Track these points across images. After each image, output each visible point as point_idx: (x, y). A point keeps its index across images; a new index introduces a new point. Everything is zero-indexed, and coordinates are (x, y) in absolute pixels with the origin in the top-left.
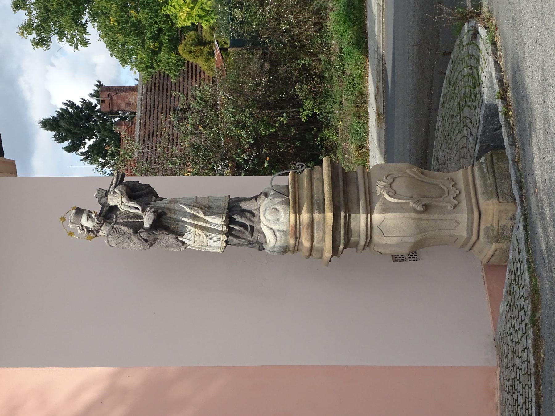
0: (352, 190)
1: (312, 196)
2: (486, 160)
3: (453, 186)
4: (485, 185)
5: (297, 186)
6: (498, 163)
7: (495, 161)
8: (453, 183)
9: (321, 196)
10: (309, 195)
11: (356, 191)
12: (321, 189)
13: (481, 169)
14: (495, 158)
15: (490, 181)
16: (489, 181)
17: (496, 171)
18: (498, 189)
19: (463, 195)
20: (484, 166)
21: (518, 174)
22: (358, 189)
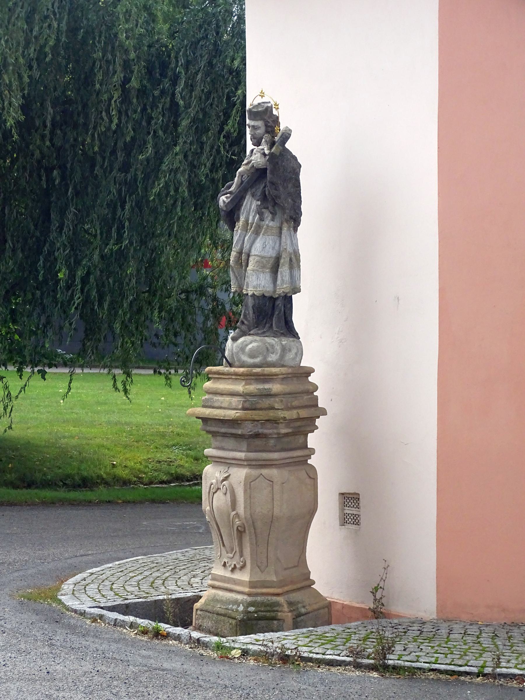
0: (230, 443)
1: (222, 394)
2: (237, 611)
3: (235, 565)
4: (221, 601)
5: (233, 377)
6: (228, 624)
7: (231, 621)
8: (238, 566)
9: (216, 404)
10: (219, 391)
11: (230, 448)
12: (223, 405)
13: (236, 602)
14: (234, 622)
15: (218, 607)
16: (219, 606)
17: (223, 618)
18: (208, 614)
19: (228, 574)
20: (235, 607)
21: (89, 616)
22: (232, 450)
